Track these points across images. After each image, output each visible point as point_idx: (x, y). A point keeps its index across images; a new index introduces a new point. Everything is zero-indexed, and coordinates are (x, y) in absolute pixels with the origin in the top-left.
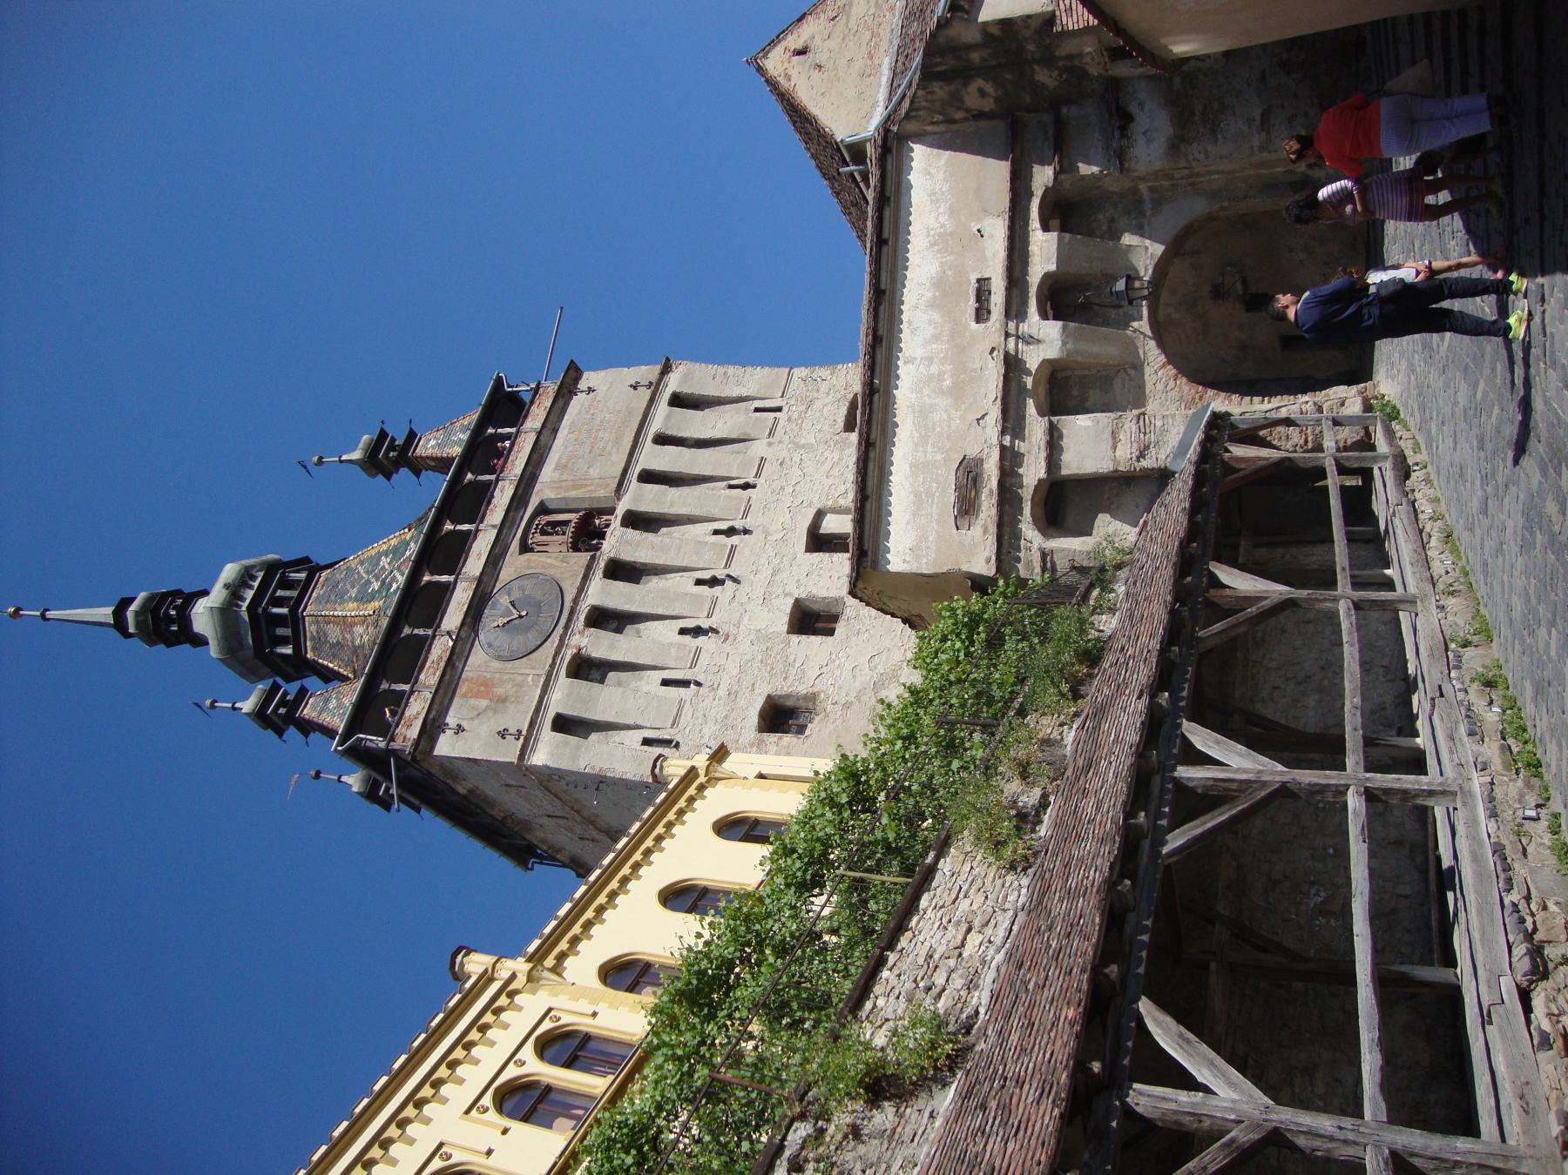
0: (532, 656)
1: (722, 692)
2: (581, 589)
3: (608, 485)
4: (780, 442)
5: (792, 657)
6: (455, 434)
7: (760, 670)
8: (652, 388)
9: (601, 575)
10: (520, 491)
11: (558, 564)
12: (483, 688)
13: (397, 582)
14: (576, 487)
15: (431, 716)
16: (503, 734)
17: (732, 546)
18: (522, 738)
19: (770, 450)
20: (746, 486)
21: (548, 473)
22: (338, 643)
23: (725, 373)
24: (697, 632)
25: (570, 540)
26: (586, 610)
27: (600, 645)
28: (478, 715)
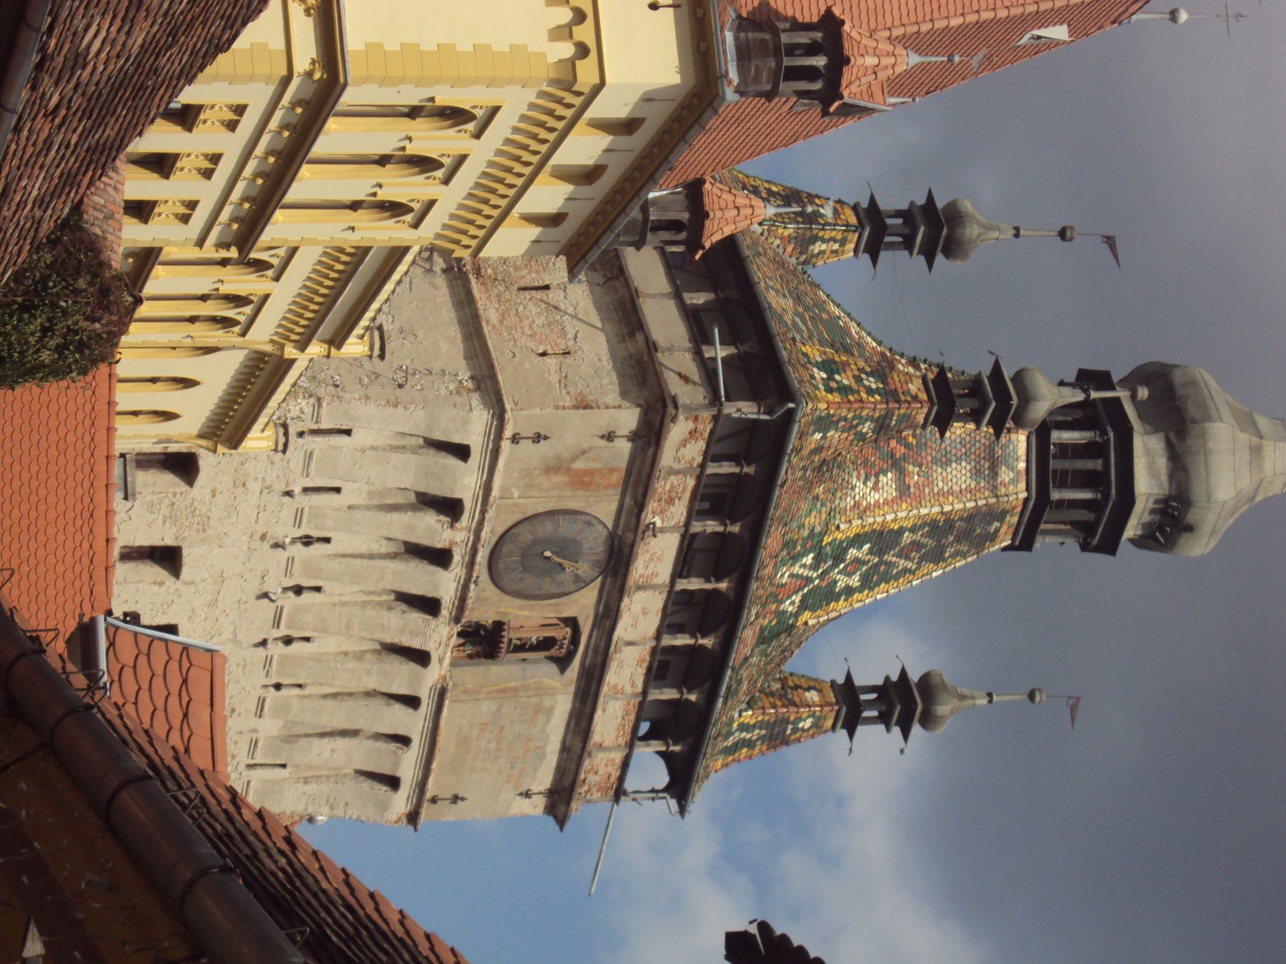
0: (518, 517)
1: (255, 487)
2: (465, 589)
3: (465, 692)
4: (241, 733)
5: (168, 523)
6: (760, 738)
7: (209, 510)
8: (428, 795)
9: (443, 602)
10: (594, 686)
11: (510, 610)
12: (586, 479)
13: (804, 566)
14: (515, 690)
15: (651, 451)
16: (538, 438)
17: (278, 627)
18: (508, 433)
19: (253, 726)
20: (278, 687)
21: (563, 704)
22: (948, 463)
23: (332, 808)
24: (307, 541)
25: (503, 633)
26: (453, 565)
27: (431, 529)
28: (584, 452)
